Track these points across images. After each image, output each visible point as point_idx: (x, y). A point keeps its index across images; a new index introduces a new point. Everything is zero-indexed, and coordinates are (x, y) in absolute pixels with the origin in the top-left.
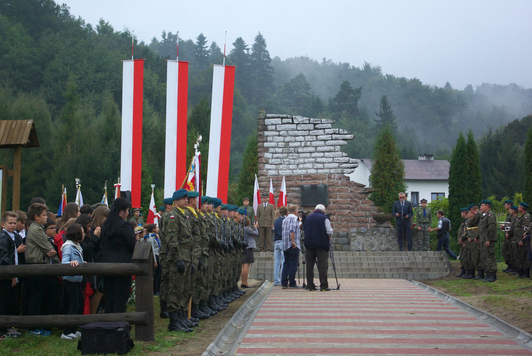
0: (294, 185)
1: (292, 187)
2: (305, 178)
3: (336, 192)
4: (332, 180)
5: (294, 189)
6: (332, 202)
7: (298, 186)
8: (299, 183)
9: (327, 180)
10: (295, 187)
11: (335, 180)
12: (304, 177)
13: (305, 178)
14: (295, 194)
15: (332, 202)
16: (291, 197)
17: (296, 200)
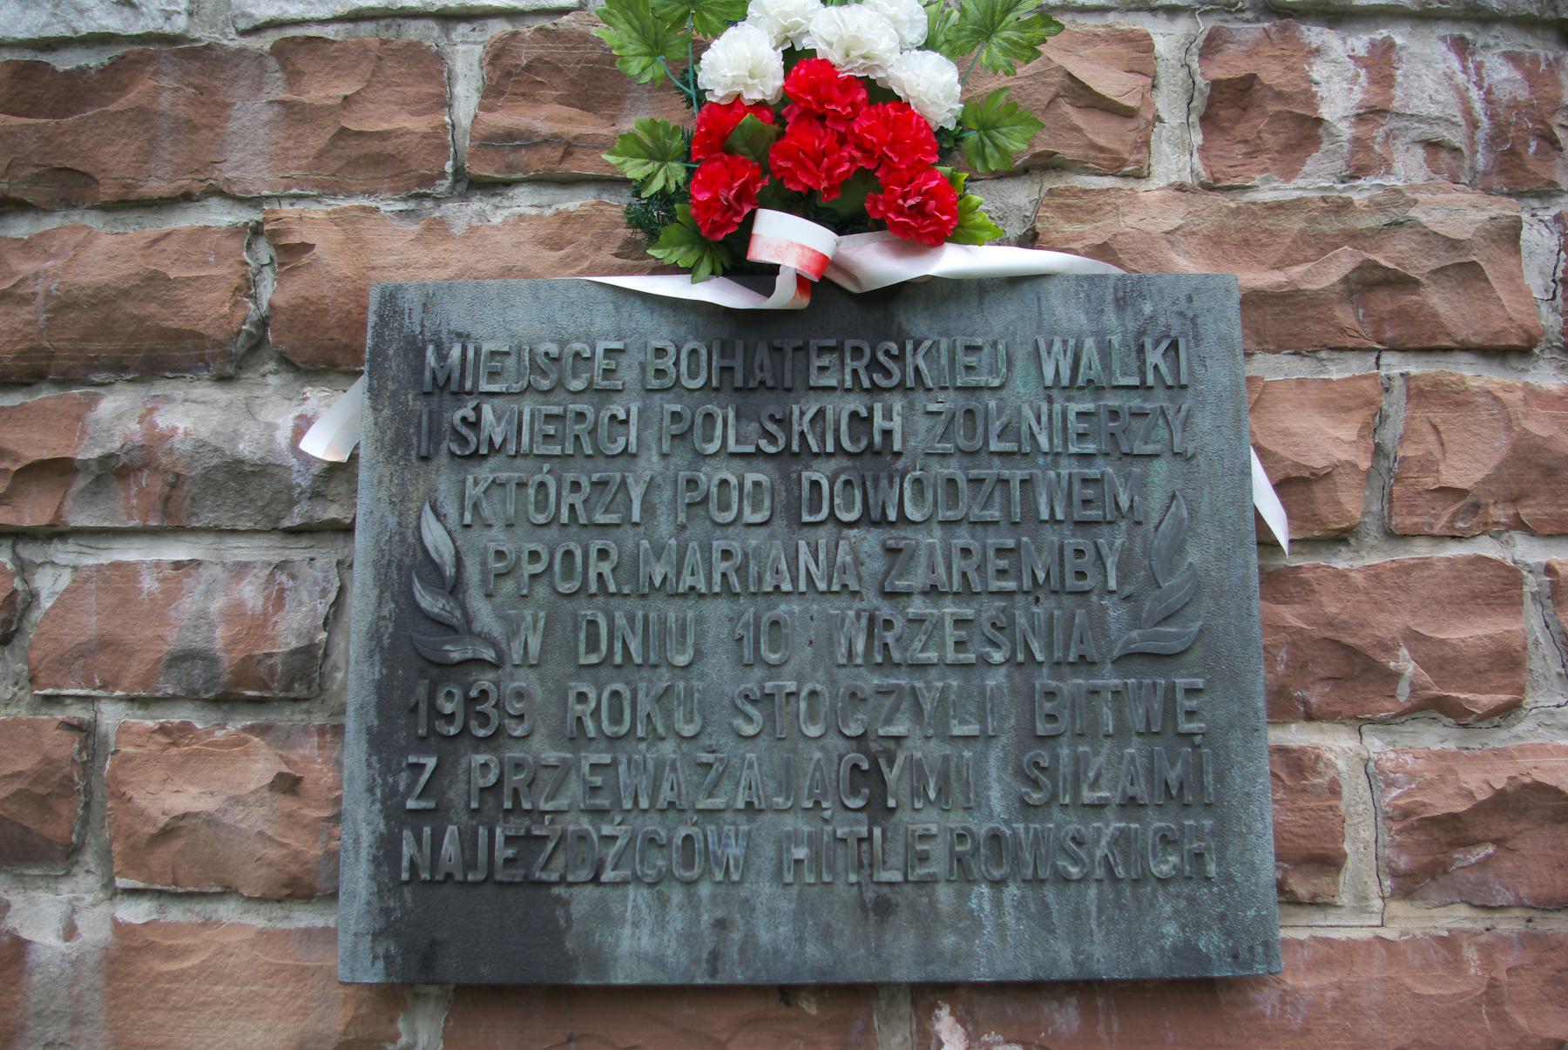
0: (209, 308)
1: (160, 357)
2: (543, 117)
3: (1468, 510)
4: (1315, 178)
5: (190, 416)
6: (1362, 841)
7: (316, 350)
8: (379, 248)
9: (1174, 158)
10: (228, 359)
11: (1408, 167)
12: (507, 77)
13: (543, 117)
14: (217, 589)
15: (1362, 841)
16: (98, 659)
17: (220, 783)
